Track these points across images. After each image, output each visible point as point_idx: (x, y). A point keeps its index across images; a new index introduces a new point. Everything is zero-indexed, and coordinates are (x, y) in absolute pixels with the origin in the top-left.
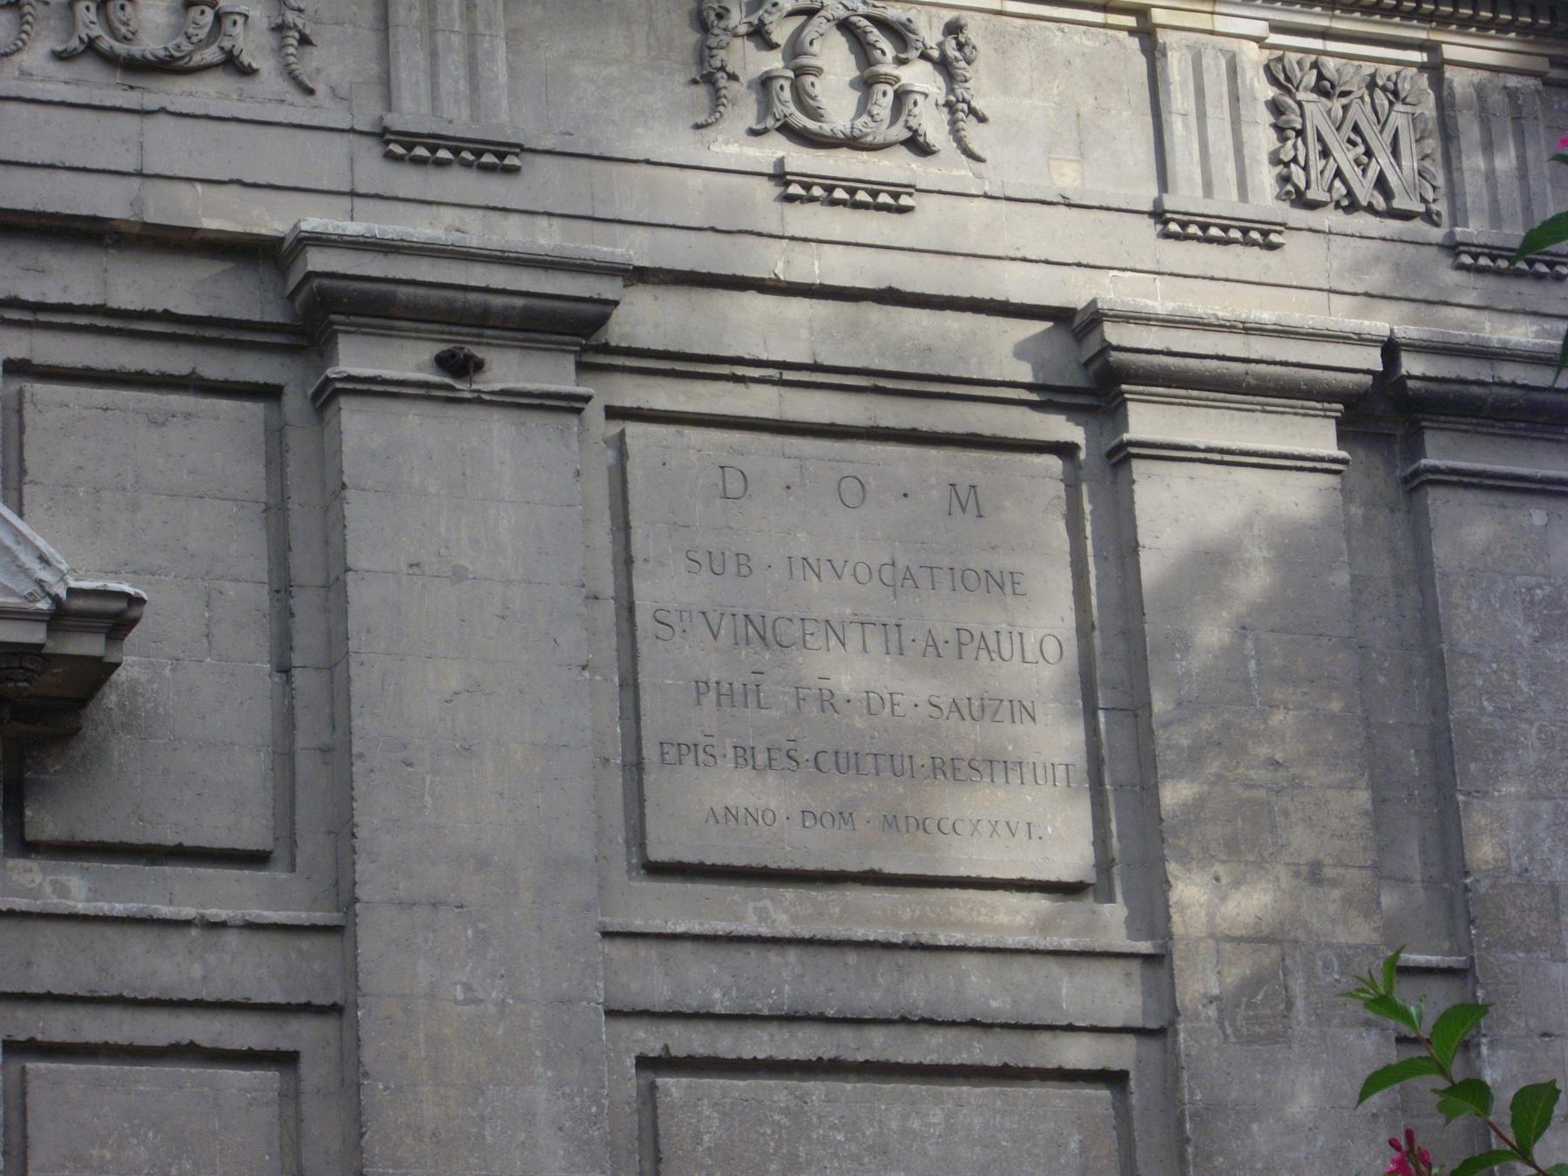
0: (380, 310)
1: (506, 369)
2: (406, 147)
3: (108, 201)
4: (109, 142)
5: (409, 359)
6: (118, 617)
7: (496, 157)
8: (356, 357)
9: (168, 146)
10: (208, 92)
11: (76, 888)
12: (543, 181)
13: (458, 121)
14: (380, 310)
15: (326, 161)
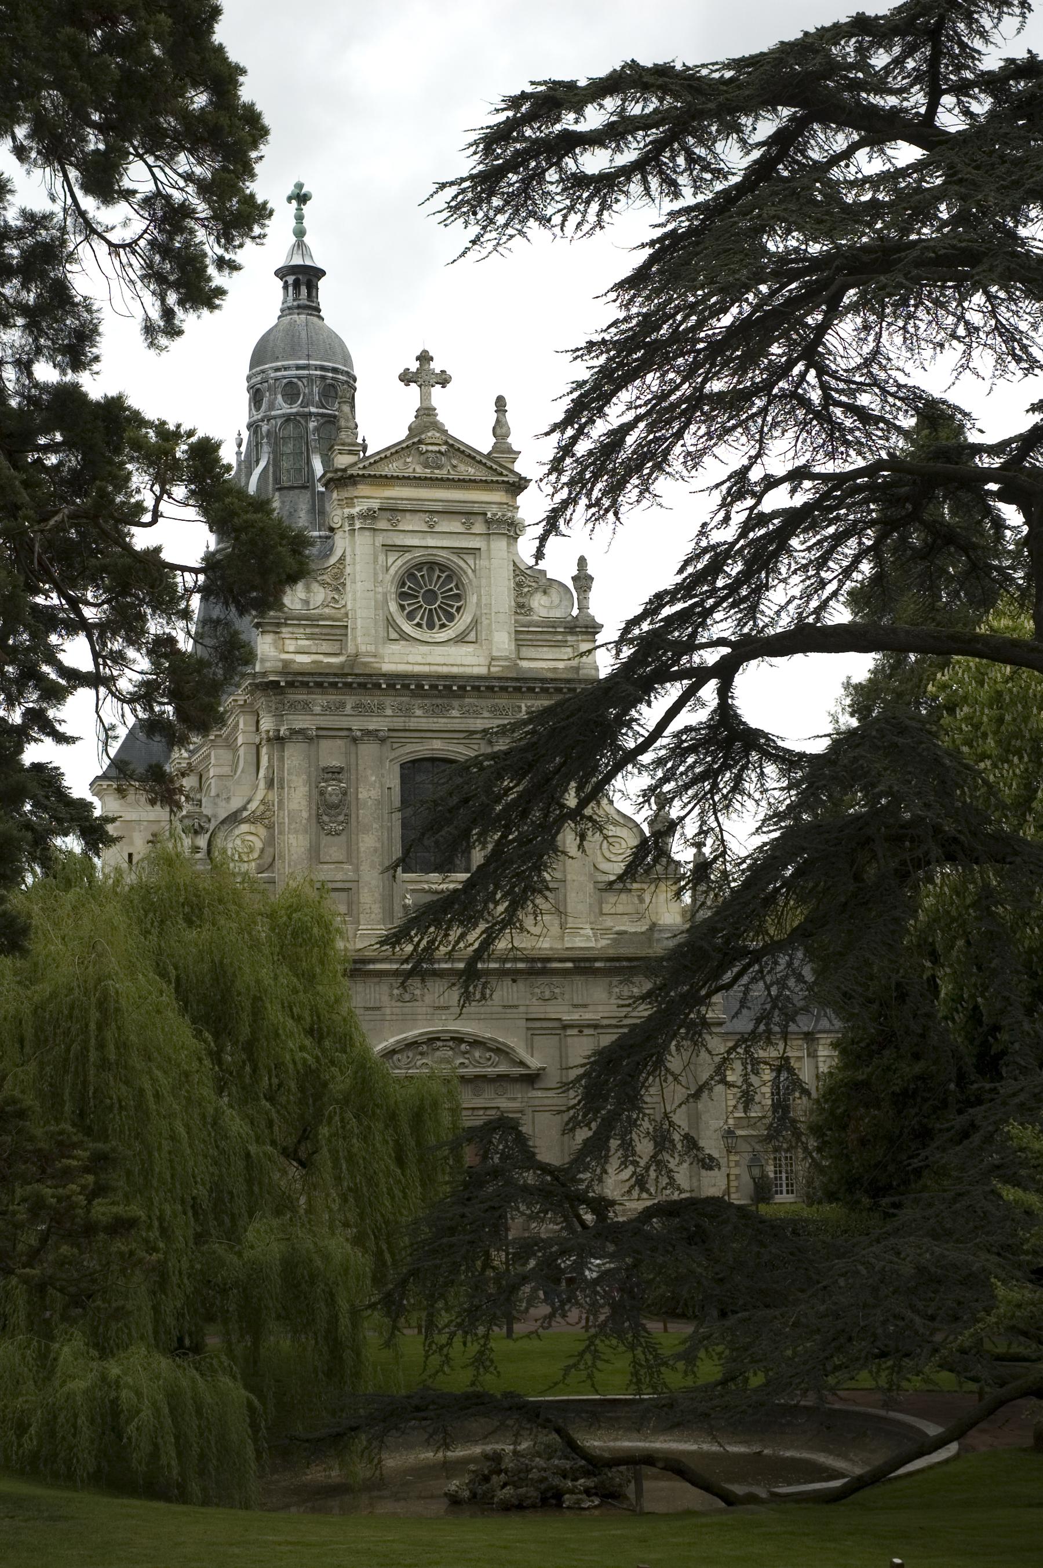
0: (572, 1026)
1: (586, 1031)
2: (575, 1006)
3: (542, 1016)
4: (542, 1009)
5: (575, 1032)
6: (544, 1069)
7: (585, 1006)
8: (569, 1032)
9: (549, 1009)
10: (553, 1002)
11: (539, 1094)
12: (591, 1008)
13: (580, 1002)
14: (572, 1026)
15: (566, 1008)
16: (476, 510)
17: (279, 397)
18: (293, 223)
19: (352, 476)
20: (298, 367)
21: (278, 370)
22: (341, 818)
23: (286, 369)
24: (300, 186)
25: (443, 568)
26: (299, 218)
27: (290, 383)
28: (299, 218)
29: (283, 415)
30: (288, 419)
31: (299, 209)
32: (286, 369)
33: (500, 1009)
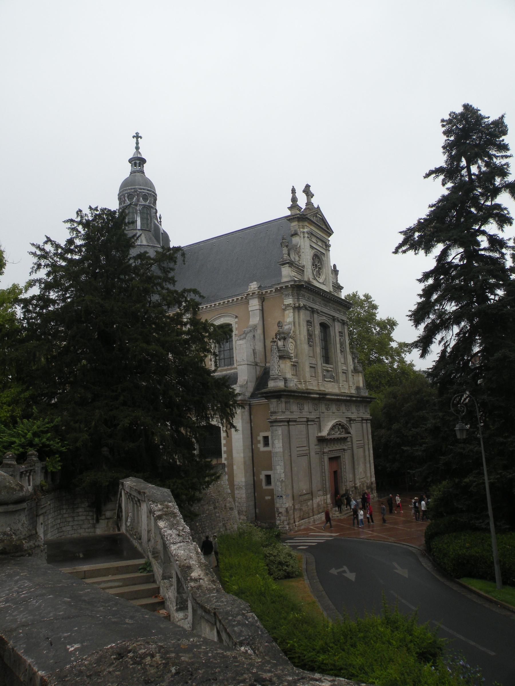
16: (325, 241)
17: (141, 198)
18: (135, 145)
19: (307, 218)
20: (148, 190)
21: (141, 189)
22: (312, 340)
23: (144, 189)
24: (137, 133)
25: (319, 258)
26: (137, 143)
27: (145, 195)
28: (137, 143)
29: (143, 205)
30: (144, 206)
31: (137, 141)
32: (144, 189)
33: (342, 414)
